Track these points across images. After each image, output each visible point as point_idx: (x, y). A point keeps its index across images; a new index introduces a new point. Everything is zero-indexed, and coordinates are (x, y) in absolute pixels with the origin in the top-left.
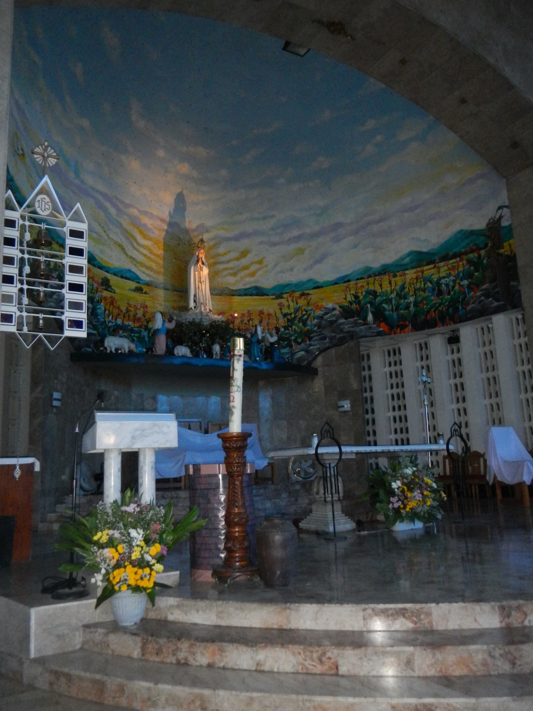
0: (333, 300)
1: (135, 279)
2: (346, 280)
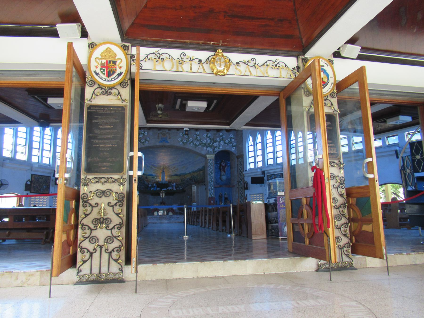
0: (188, 177)
1: (152, 175)
2: (190, 173)
